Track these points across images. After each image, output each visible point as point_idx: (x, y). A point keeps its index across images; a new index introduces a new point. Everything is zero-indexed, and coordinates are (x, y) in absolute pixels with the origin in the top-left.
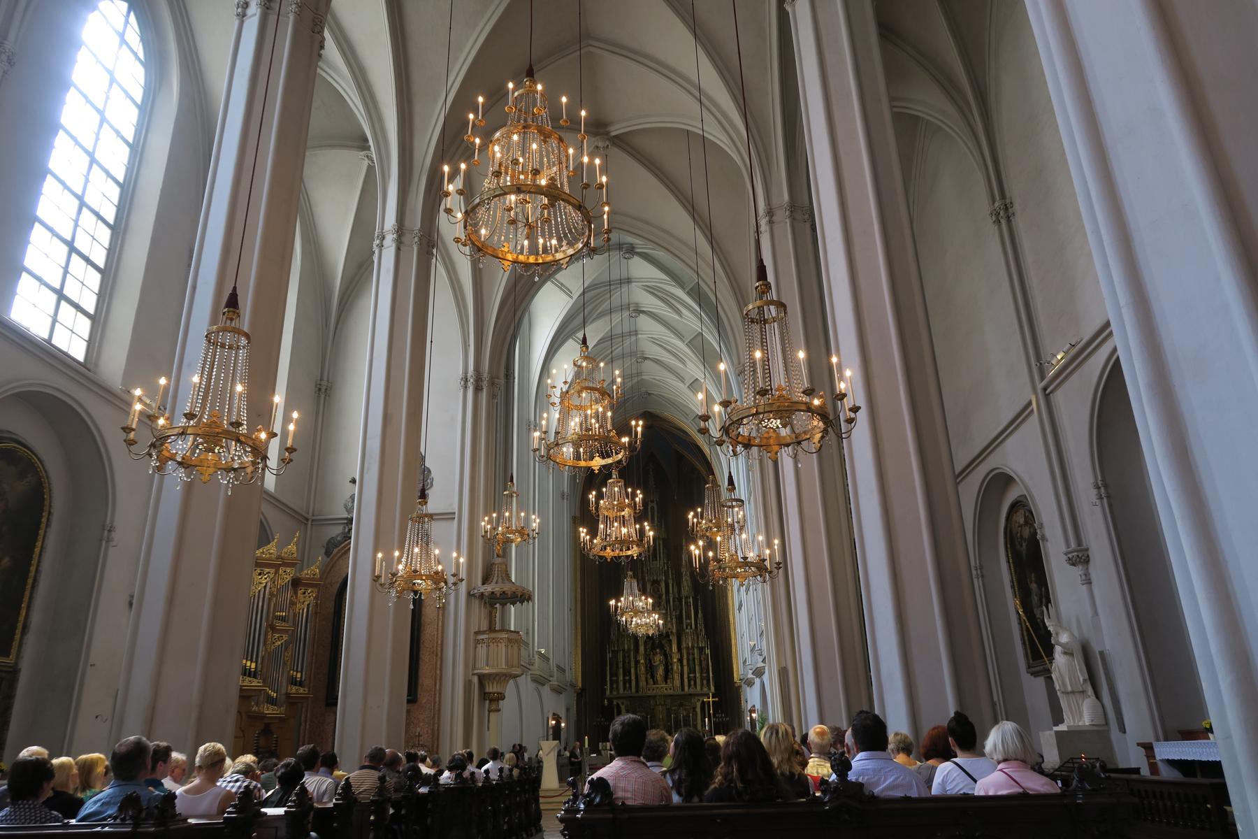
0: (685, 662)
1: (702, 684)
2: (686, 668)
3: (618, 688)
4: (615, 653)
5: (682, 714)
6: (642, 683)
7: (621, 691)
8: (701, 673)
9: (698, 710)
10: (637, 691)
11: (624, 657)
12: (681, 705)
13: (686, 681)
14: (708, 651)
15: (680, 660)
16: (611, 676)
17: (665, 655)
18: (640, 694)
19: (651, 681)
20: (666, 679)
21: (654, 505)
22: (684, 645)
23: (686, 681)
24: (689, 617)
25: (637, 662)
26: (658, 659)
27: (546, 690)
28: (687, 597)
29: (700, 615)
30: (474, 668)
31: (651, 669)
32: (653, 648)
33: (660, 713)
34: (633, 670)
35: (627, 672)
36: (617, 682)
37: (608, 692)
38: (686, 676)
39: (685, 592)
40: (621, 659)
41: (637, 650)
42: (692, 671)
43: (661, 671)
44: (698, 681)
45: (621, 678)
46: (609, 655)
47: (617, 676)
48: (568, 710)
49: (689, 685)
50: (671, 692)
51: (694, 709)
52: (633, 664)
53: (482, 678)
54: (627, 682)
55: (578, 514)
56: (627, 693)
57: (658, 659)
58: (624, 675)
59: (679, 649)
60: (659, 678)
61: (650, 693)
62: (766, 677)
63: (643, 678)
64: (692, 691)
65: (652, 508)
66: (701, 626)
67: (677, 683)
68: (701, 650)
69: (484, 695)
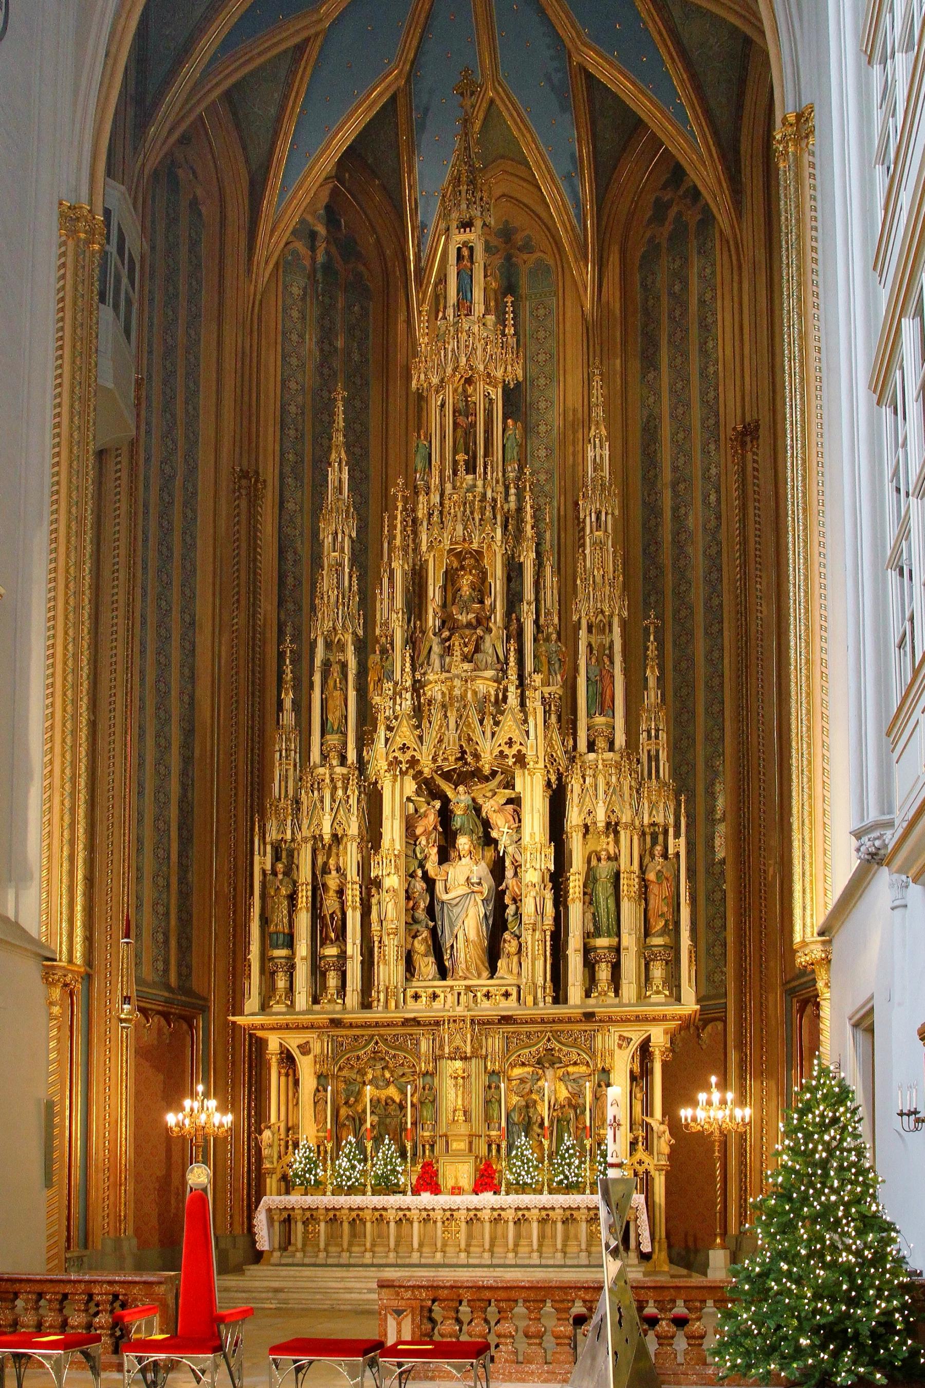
6: (389, 971)
7: (302, 1000)
10: (366, 1005)
12: (547, 1060)
14: (678, 845)
16: (267, 940)
18: (377, 1014)
19: (426, 965)
20: (493, 954)
22: (574, 817)
24: (601, 702)
25: (371, 885)
28: (600, 627)
29: (652, 696)
34: (353, 919)
35: (328, 928)
39: (583, 611)
40: (305, 874)
43: (467, 926)
45: (303, 949)
46: (262, 861)
47: (290, 942)
50: (509, 1007)
51: (605, 1072)
52: (353, 894)
56: (330, 1008)
58: (318, 938)
61: (415, 1009)
67: (537, 968)
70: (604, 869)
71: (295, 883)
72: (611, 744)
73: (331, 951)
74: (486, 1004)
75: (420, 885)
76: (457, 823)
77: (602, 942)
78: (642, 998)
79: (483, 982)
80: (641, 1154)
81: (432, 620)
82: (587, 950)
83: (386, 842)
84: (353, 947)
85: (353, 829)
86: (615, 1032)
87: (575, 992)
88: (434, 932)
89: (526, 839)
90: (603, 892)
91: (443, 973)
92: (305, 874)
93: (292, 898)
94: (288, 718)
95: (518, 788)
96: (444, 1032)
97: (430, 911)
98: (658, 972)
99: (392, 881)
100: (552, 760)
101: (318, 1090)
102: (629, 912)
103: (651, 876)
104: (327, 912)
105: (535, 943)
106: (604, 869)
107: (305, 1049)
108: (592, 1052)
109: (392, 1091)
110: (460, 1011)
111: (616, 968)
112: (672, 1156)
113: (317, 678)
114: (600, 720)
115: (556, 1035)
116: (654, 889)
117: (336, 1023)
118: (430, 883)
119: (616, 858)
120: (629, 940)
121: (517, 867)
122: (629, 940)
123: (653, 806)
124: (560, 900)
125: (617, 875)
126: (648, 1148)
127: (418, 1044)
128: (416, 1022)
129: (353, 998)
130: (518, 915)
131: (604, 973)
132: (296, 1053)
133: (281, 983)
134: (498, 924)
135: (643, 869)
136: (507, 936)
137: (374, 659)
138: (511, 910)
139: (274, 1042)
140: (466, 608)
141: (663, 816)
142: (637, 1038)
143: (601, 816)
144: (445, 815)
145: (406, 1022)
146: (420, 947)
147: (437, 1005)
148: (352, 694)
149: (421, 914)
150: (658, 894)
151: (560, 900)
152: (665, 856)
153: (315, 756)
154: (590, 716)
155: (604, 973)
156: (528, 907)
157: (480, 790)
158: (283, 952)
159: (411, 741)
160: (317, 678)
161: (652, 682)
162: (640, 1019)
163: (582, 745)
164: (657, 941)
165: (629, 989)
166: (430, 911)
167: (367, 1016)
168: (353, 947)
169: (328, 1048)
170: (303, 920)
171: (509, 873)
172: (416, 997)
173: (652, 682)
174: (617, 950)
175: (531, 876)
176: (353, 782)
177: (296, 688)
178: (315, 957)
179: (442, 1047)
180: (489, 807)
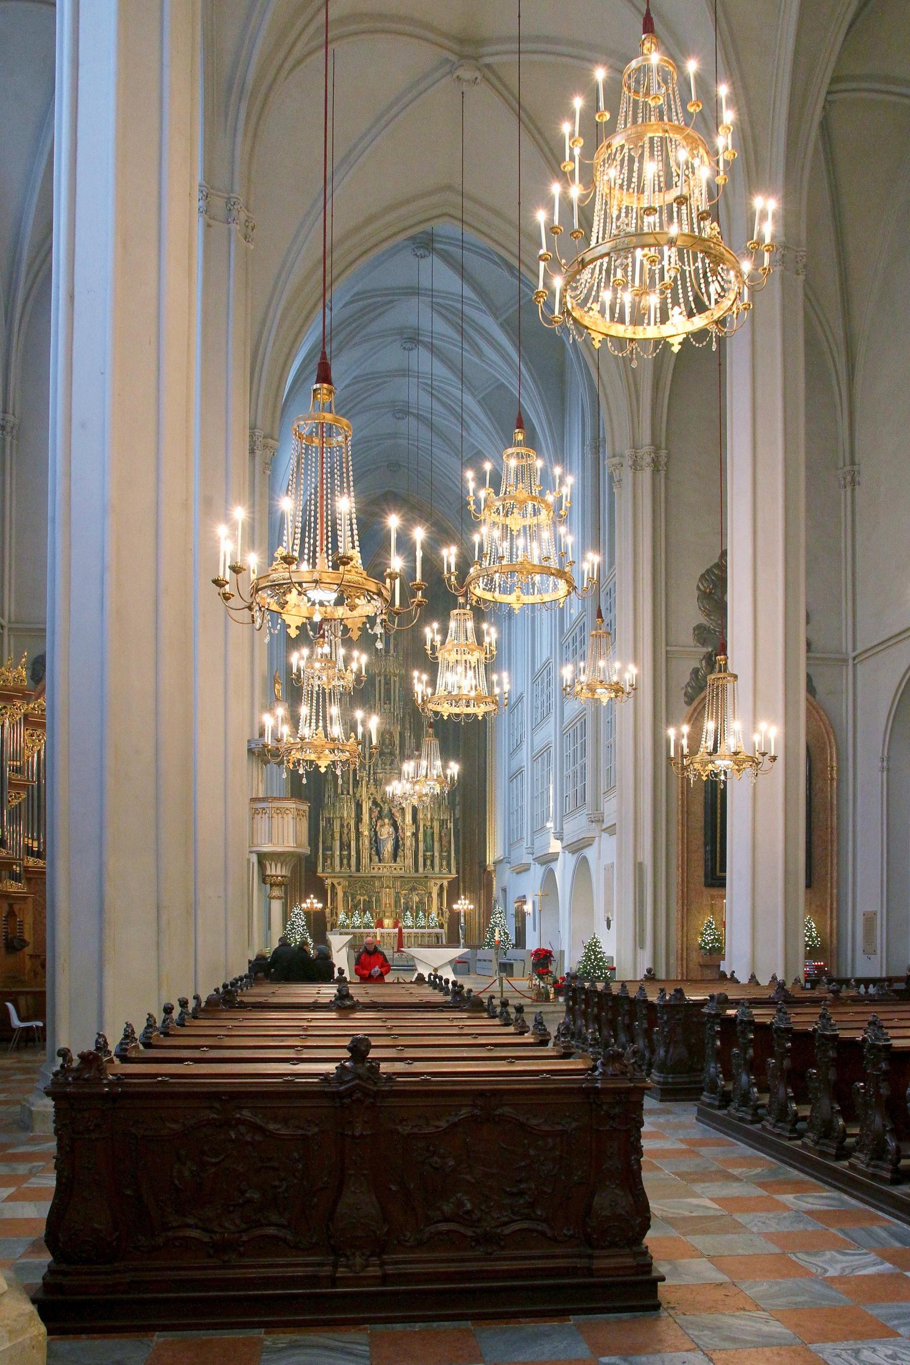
0: (421, 836)
1: (441, 866)
2: (421, 845)
4: (329, 820)
5: (416, 899)
6: (365, 861)
7: (337, 869)
8: (441, 851)
10: (358, 870)
11: (342, 826)
12: (413, 889)
13: (421, 860)
14: (451, 825)
15: (415, 835)
17: (395, 825)
18: (362, 874)
19: (376, 858)
20: (395, 856)
23: (421, 860)
25: (358, 834)
26: (386, 832)
30: (252, 844)
31: (376, 842)
32: (380, 817)
33: (387, 898)
36: (332, 856)
37: (320, 869)
38: (421, 854)
40: (337, 829)
41: (359, 819)
42: (429, 848)
43: (388, 847)
44: (437, 861)
46: (322, 824)
47: (331, 849)
49: (425, 865)
51: (430, 893)
52: (353, 835)
53: (262, 858)
54: (345, 859)
57: (386, 832)
60: (386, 856)
61: (375, 872)
62: (552, 865)
63: (365, 854)
67: (410, 861)
68: (443, 823)
69: (264, 878)
70: (429, 831)
73: (345, 853)
75: (373, 833)
77: (428, 854)
80: (440, 917)
83: (364, 821)
84: (353, 853)
85: (353, 816)
86: (433, 881)
87: (421, 869)
88: (377, 847)
90: (429, 839)
91: (380, 861)
92: (337, 829)
93: (332, 835)
97: (376, 841)
98: (444, 863)
99: (366, 833)
102: (436, 845)
105: (409, 853)
106: (429, 831)
107: (339, 884)
109: (366, 897)
111: (432, 862)
117: (350, 876)
118: (376, 833)
119: (432, 828)
120: (436, 854)
121: (403, 829)
124: (417, 841)
125: (433, 833)
129: (353, 868)
131: (428, 862)
132: (336, 885)
134: (396, 847)
135: (440, 832)
138: (401, 842)
139: (329, 881)
140: (387, 747)
141: (444, 816)
142: (439, 883)
144: (380, 812)
145: (372, 877)
146: (373, 853)
147: (380, 871)
153: (339, 791)
155: (428, 862)
156: (408, 843)
159: (374, 792)
162: (440, 878)
164: (445, 854)
165: (437, 869)
166: (376, 841)
167: (358, 874)
168: (353, 853)
170: (338, 843)
171: (400, 831)
174: (433, 856)
180: (394, 810)
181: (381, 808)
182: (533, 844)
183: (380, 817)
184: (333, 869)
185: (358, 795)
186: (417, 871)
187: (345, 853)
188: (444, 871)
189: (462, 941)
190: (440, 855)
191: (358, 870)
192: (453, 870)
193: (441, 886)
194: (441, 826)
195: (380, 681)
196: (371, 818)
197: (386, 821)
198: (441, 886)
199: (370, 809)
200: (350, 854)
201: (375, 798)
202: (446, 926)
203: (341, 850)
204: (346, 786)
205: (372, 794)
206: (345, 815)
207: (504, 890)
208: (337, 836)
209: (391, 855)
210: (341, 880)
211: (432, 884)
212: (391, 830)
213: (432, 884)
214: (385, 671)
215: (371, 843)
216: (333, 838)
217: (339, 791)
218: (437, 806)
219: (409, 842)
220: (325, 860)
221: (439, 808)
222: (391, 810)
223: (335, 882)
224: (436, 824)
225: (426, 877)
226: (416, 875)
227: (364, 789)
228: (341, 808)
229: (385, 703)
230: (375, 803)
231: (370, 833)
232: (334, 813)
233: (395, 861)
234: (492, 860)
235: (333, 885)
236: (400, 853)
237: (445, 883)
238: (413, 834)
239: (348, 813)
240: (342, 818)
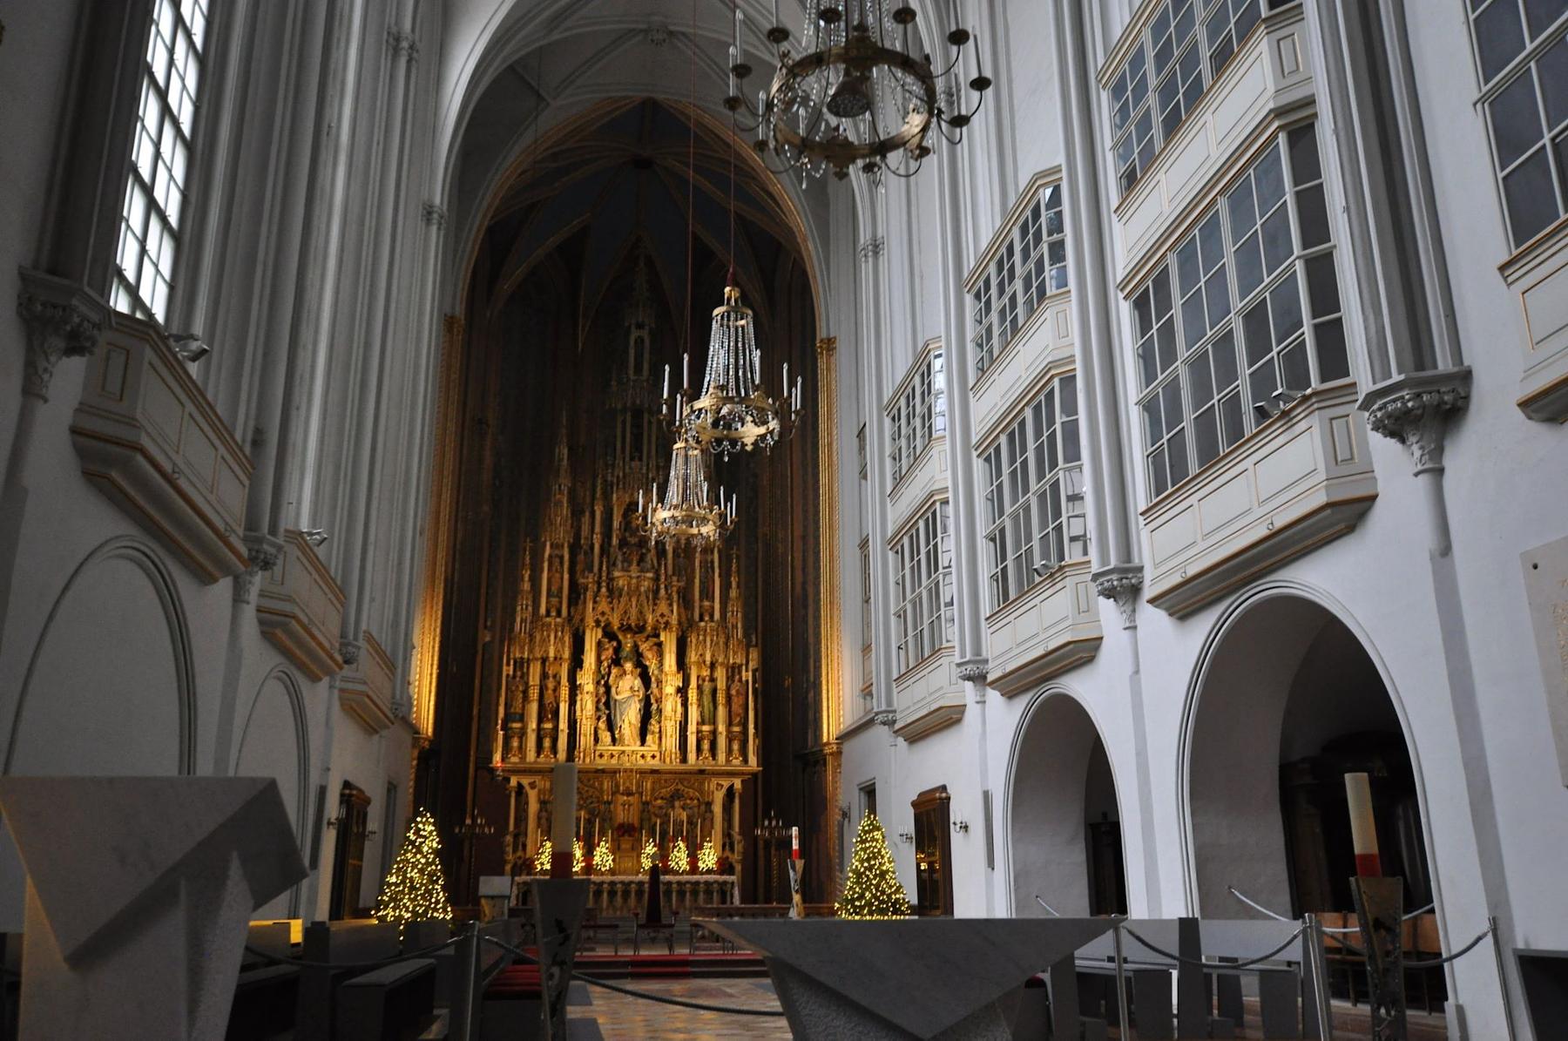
0: (692, 694)
1: (730, 752)
3: (522, 749)
4: (520, 664)
6: (586, 740)
7: (531, 755)
8: (730, 724)
9: (717, 809)
10: (570, 757)
11: (544, 676)
13: (692, 740)
14: (747, 675)
15: (682, 691)
19: (605, 736)
21: (645, 333)
22: (692, 657)
23: (692, 740)
24: (707, 594)
25: (574, 689)
26: (627, 686)
27: (320, 698)
29: (733, 593)
31: (607, 705)
32: (617, 662)
35: (548, 712)
36: (523, 734)
37: (497, 757)
38: (692, 728)
40: (534, 679)
41: (577, 663)
42: (709, 718)
43: (630, 717)
46: (508, 670)
47: (522, 718)
48: (392, 788)
49: (699, 749)
50: (655, 764)
51: (709, 804)
52: (564, 692)
55: (460, 311)
56: (545, 760)
57: (627, 686)
58: (540, 721)
59: (682, 665)
61: (602, 763)
63: (586, 726)
64: (707, 764)
65: (640, 341)
66: (736, 618)
67: (671, 742)
68: (733, 671)
70: (707, 686)
71: (527, 683)
72: (712, 616)
73: (548, 726)
74: (642, 762)
75: (602, 690)
76: (624, 654)
77: (706, 728)
78: (728, 761)
79: (637, 747)
80: (728, 853)
81: (615, 541)
82: (698, 732)
83: (586, 665)
84: (563, 725)
85: (567, 655)
86: (714, 781)
88: (609, 717)
89: (666, 668)
90: (707, 700)
91: (614, 741)
92: (534, 679)
93: (525, 692)
94: (526, 586)
95: (662, 638)
96: (620, 778)
97: (607, 704)
98: (736, 747)
100: (680, 623)
101: (541, 810)
102: (721, 712)
103: (733, 692)
104: (547, 701)
107: (532, 786)
108: (701, 792)
110: (628, 765)
112: (744, 853)
113: (546, 565)
114: (706, 603)
115: (681, 781)
116: (735, 699)
118: (608, 688)
119: (713, 680)
120: (721, 728)
121: (659, 682)
122: (721, 728)
123: (735, 653)
124: (685, 704)
125: (714, 691)
126: (732, 849)
127: (601, 784)
128: (603, 771)
130: (660, 711)
131: (706, 745)
132: (527, 788)
133: (515, 743)
135: (728, 688)
136: (653, 721)
137: (581, 557)
138: (654, 707)
139: (513, 781)
142: (726, 783)
143: (708, 658)
144: (617, 650)
145: (597, 771)
146: (602, 725)
147: (614, 761)
148: (566, 576)
149: (602, 706)
150: (737, 704)
151: (685, 704)
152: (740, 680)
153: (543, 610)
154: (701, 600)
157: (640, 638)
158: (517, 725)
159: (607, 610)
160: (546, 565)
161: (734, 585)
163: (697, 617)
164: (736, 729)
165: (721, 757)
166: (607, 704)
168: (563, 725)
169: (548, 784)
170: (534, 708)
171: (654, 685)
172: (601, 756)
173: (734, 585)
174: (714, 733)
175: (670, 689)
176: (567, 628)
177: (533, 570)
178: (539, 729)
179: (617, 786)
180: (644, 647)
181: (619, 643)
182: (977, 650)
183: (617, 662)
184: (523, 758)
185: (577, 619)
186: (684, 760)
187: (548, 726)
188: (735, 762)
189: (797, 898)
190: (729, 731)
191: (570, 757)
192: (753, 760)
193: (731, 789)
194: (730, 679)
195: (624, 422)
196: (599, 662)
197: (628, 666)
198: (731, 789)
199: (599, 644)
200: (556, 728)
201: (608, 624)
202: (738, 868)
203: (540, 721)
204: (554, 600)
205: (603, 614)
206: (552, 654)
207: (870, 792)
208: (534, 694)
209: (636, 732)
210: (537, 779)
211: (713, 786)
212: (638, 683)
213: (713, 786)
214: (634, 403)
215: (597, 709)
216: (526, 698)
217: (543, 610)
218: (722, 641)
219: (671, 705)
220: (507, 740)
221: (726, 644)
222: (636, 647)
223: (525, 782)
224: (720, 674)
225: (702, 772)
226: (683, 767)
227: (590, 605)
228: (545, 641)
229: (632, 459)
230: (609, 634)
231: (597, 689)
232: (531, 651)
233: (643, 742)
234: (834, 733)
235: (520, 786)
236: (654, 726)
237: (738, 784)
238: (679, 690)
239: (557, 651)
240: (544, 660)
